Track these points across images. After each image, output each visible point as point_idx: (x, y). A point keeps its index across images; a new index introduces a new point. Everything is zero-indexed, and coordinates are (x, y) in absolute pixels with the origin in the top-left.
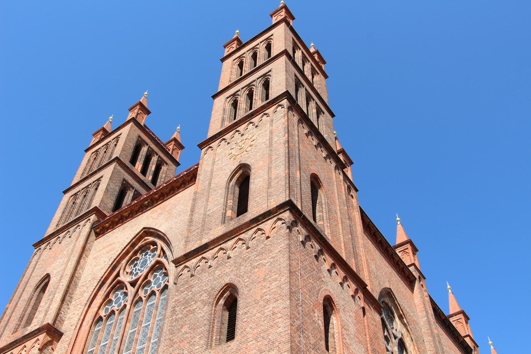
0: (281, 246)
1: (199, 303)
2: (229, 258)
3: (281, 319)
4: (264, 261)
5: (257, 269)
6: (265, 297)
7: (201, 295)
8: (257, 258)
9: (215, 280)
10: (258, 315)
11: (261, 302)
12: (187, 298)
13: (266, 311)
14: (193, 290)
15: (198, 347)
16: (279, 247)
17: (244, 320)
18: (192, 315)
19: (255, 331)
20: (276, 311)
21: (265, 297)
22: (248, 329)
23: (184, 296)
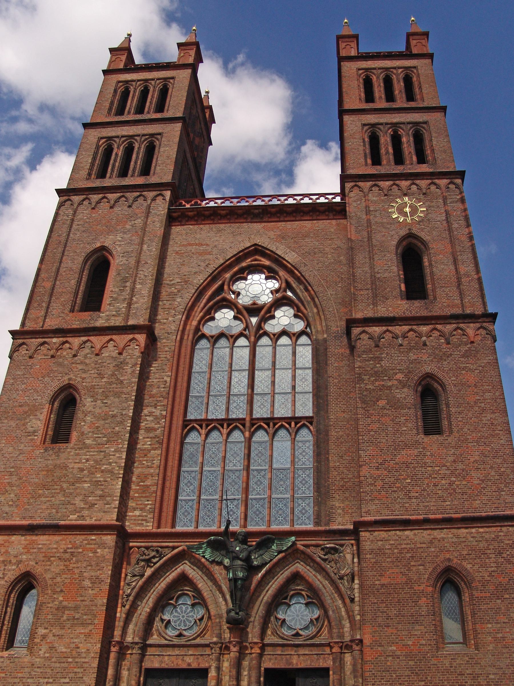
1: (396, 382)
2: (425, 344)
8: (462, 359)
12: (376, 369)
15: (405, 429)
18: (388, 392)
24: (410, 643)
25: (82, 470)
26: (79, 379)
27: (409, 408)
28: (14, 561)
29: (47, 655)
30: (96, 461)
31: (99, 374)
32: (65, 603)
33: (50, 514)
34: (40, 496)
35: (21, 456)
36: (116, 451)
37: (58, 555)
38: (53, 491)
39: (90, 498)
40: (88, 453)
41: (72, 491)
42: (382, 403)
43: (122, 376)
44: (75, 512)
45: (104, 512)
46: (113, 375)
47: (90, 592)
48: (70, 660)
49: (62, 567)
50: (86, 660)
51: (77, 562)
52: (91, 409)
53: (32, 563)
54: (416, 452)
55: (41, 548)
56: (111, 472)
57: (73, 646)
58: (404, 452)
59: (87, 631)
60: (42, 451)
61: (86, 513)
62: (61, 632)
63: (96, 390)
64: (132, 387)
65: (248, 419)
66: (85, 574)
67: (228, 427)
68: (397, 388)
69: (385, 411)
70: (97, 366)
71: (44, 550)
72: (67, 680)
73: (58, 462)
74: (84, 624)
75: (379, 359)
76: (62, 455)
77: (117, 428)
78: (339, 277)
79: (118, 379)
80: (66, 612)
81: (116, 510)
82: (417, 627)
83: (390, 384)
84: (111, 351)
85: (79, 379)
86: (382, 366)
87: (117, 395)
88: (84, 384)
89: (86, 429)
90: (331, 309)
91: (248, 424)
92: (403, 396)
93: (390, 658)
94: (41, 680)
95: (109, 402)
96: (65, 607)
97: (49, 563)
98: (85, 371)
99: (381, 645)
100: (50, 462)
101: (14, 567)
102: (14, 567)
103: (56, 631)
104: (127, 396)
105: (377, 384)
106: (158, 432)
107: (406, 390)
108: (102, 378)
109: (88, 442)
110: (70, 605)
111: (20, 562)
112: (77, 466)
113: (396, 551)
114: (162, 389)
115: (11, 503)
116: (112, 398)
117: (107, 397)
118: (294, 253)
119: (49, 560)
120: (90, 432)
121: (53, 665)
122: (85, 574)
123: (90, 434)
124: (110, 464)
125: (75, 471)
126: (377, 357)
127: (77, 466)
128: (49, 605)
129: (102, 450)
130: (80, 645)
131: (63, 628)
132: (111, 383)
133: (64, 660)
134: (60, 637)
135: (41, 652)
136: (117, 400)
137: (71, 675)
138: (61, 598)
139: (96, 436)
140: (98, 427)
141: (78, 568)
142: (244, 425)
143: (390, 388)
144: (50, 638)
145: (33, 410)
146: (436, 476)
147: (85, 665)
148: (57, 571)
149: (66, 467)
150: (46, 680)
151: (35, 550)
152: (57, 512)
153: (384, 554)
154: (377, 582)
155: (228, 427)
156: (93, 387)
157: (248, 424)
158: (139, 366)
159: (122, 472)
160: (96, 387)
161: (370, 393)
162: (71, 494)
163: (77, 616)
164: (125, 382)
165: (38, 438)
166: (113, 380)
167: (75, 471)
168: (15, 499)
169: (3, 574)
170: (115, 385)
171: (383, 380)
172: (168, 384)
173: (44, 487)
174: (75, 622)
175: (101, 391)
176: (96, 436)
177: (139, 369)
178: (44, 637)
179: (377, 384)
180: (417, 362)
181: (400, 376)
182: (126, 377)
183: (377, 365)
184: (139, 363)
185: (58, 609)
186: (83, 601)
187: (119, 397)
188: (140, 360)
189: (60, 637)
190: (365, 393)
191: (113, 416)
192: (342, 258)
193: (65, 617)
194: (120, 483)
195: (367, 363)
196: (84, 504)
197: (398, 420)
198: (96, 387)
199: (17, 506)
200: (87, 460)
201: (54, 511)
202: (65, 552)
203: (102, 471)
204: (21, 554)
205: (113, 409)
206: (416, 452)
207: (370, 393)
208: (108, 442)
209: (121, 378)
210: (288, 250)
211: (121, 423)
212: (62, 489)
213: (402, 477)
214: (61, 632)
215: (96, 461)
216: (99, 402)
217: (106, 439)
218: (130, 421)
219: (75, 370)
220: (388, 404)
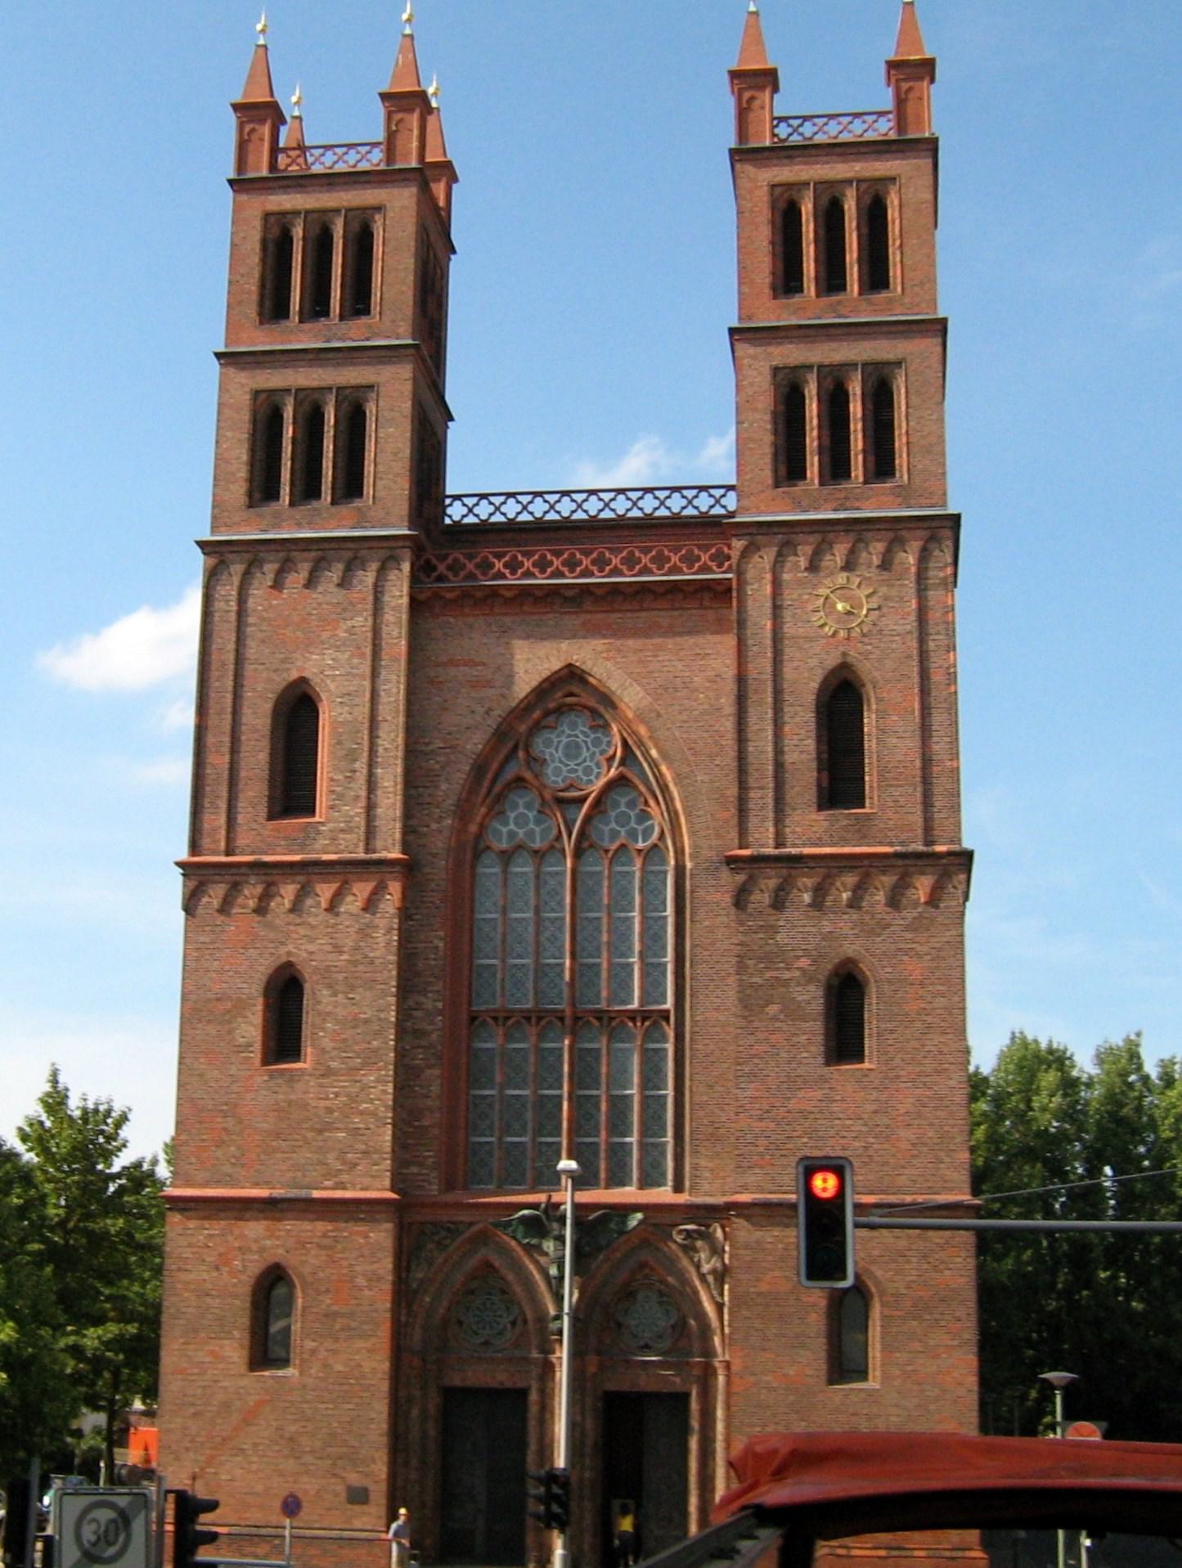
0: (951, 933)
1: (797, 973)
3: (952, 1067)
4: (924, 949)
5: (906, 958)
6: (925, 1018)
7: (799, 957)
9: (823, 939)
10: (915, 1044)
11: (918, 1024)
12: (768, 948)
13: (928, 1042)
14: (778, 937)
15: (805, 1055)
16: (947, 933)
17: (890, 1042)
18: (784, 990)
19: (910, 1068)
20: (945, 1050)
21: (925, 1018)
22: (897, 1061)
23: (762, 942)
24: (792, 1373)
25: (330, 1111)
26: (305, 955)
27: (815, 1020)
28: (254, 1247)
29: (321, 1375)
30: (348, 1095)
31: (335, 946)
32: (335, 1308)
33: (294, 1178)
34: (275, 1150)
35: (235, 1085)
36: (378, 1081)
37: (315, 1240)
38: (294, 1143)
39: (350, 1155)
40: (336, 1084)
41: (321, 1144)
42: (773, 1009)
43: (374, 950)
44: (328, 1175)
45: (372, 1176)
46: (357, 948)
47: (367, 1293)
48: (352, 1381)
49: (323, 1258)
50: (373, 1382)
51: (342, 1252)
52: (330, 1008)
53: (281, 1251)
54: (819, 1094)
55: (289, 1230)
56: (374, 1114)
57: (353, 1363)
58: (801, 1094)
59: (369, 1345)
60: (266, 1078)
61: (345, 1177)
62: (336, 1346)
63: (334, 975)
64: (390, 971)
65: (568, 1013)
66: (358, 1268)
67: (538, 1023)
68: (799, 984)
69: (778, 1024)
70: (329, 930)
71: (294, 1233)
72: (351, 1406)
73: (293, 1097)
74: (362, 1336)
75: (772, 930)
76: (298, 1086)
77: (375, 1043)
78: (716, 743)
79: (366, 957)
80: (340, 1320)
81: (388, 1174)
82: (802, 1352)
83: (787, 975)
84: (352, 904)
85: (305, 955)
86: (777, 944)
87: (370, 984)
88: (314, 963)
89: (327, 1043)
90: (701, 813)
91: (568, 1022)
92: (806, 997)
93: (764, 1391)
94: (320, 1406)
95: (358, 997)
96: (336, 1314)
97: (304, 1252)
98: (311, 940)
99: (753, 1374)
100: (281, 1097)
101: (256, 1257)
102: (256, 1257)
103: (329, 1344)
104: (382, 986)
105: (768, 974)
106: (434, 1036)
107: (812, 988)
108: (341, 953)
109: (334, 1064)
110: (343, 1311)
111: (262, 1250)
112: (323, 1104)
113: (780, 1246)
114: (433, 962)
115: (233, 1160)
116: (361, 990)
117: (353, 988)
118: (639, 688)
119: (304, 1247)
120: (335, 1049)
121: (331, 1387)
122: (358, 1268)
123: (336, 1052)
124: (371, 1101)
125: (321, 1113)
126: (772, 926)
127: (323, 1104)
128: (314, 1310)
129: (358, 1078)
130: (363, 1364)
131: (337, 1340)
132: (355, 963)
133: (345, 1381)
134: (335, 1352)
135: (313, 1371)
136: (368, 994)
137: (356, 1400)
138: (329, 1301)
139: (344, 1055)
140: (345, 1040)
141: (345, 1259)
142: (562, 1019)
143: (786, 983)
144: (323, 1354)
145: (240, 1006)
146: (846, 1134)
147: (372, 1388)
148: (317, 1263)
149: (305, 1106)
150: (325, 1406)
151: (282, 1233)
152: (304, 1176)
153: (763, 1250)
154: (752, 1290)
155: (538, 1023)
156: (328, 969)
157: (568, 1022)
158: (396, 932)
159: (390, 1115)
160: (334, 969)
161: (756, 990)
162: (321, 1148)
163: (354, 1324)
164: (377, 961)
165: (256, 1055)
166: (358, 957)
167: (321, 1113)
168: (238, 1154)
169: (244, 1266)
170: (361, 968)
171: (778, 969)
172: (441, 953)
173: (278, 1135)
174: (352, 1333)
175: (341, 977)
176: (344, 1055)
177: (396, 938)
178: (313, 1351)
179: (768, 974)
180: (829, 937)
181: (804, 963)
182: (378, 953)
183: (771, 941)
184: (396, 926)
185: (326, 1315)
186: (358, 1305)
187: (370, 989)
188: (396, 920)
189: (335, 1352)
190: (748, 992)
191: (367, 1021)
192: (723, 700)
193: (338, 1327)
194: (390, 1132)
195: (754, 936)
196: (343, 1164)
197: (795, 1039)
198: (334, 969)
199: (243, 1165)
200: (337, 1095)
201: (300, 1174)
202: (325, 1236)
203: (362, 1113)
204: (263, 1239)
205: (365, 1009)
206: (819, 1094)
207: (756, 990)
208: (364, 1065)
209: (372, 955)
210: (629, 681)
211: (377, 1033)
212: (307, 1142)
213: (795, 1134)
214: (336, 1346)
215: (348, 1095)
216: (340, 996)
217: (359, 1060)
218: (393, 1031)
219: (296, 936)
220: (782, 1011)
